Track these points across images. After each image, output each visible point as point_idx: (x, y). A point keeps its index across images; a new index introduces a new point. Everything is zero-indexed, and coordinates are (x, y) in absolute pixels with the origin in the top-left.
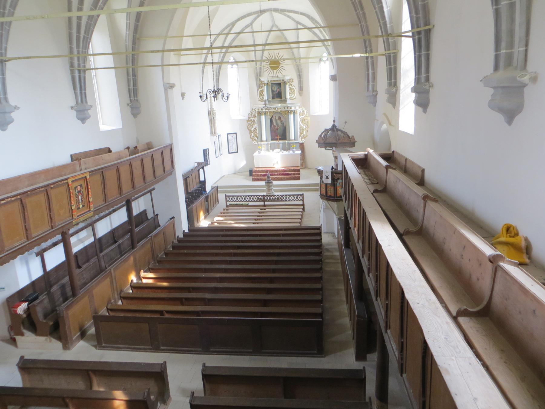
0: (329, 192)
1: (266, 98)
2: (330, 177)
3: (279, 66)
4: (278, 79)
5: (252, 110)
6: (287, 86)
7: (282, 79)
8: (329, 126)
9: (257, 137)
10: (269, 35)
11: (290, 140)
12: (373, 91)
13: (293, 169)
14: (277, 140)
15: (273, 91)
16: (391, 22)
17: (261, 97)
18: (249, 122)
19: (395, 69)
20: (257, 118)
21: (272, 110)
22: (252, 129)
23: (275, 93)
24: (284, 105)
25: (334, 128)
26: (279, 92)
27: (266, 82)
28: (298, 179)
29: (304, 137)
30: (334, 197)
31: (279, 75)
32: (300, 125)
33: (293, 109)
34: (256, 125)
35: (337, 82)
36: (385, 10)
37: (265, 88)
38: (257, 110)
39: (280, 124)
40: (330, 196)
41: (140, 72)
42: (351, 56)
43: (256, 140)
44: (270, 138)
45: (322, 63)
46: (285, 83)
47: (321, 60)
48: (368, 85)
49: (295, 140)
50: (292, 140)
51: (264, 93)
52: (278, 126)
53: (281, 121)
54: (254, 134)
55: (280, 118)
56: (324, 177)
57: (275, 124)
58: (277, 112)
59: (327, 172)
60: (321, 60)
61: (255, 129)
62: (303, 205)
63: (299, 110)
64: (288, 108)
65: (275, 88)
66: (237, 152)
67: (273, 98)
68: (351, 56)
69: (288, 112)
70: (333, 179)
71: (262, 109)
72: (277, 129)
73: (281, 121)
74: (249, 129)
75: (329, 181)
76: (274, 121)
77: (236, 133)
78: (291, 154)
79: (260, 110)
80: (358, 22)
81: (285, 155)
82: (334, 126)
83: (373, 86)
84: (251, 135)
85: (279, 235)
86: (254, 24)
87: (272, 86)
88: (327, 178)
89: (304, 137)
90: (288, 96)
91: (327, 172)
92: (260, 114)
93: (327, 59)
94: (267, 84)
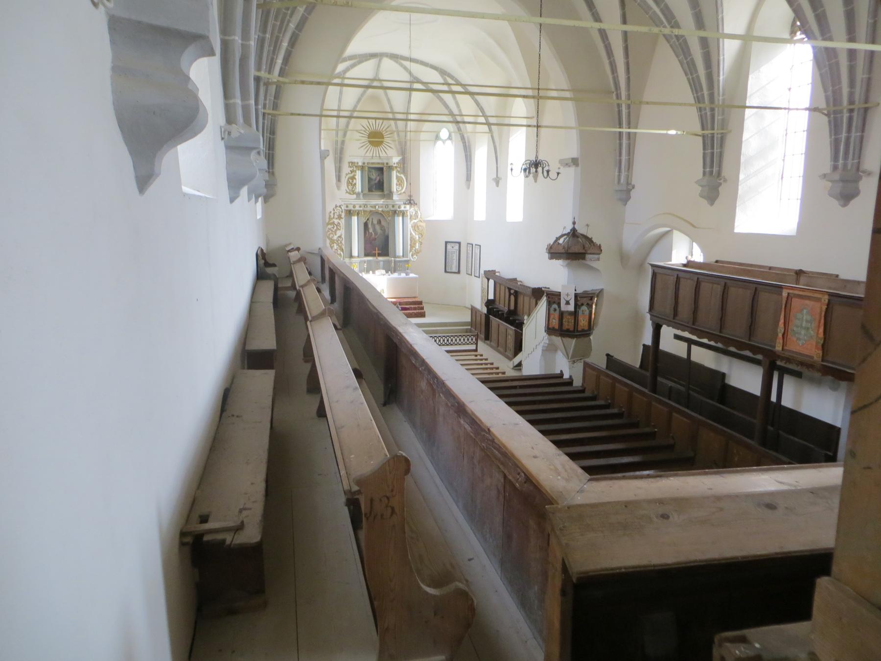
0: (565, 323)
1: (358, 188)
2: (572, 302)
3: (382, 142)
4: (379, 161)
6: (394, 174)
7: (385, 161)
8: (568, 230)
10: (364, 92)
11: (395, 257)
12: (628, 184)
13: (410, 300)
14: (374, 255)
15: (370, 179)
16: (723, 95)
17: (350, 187)
18: (330, 226)
19: (721, 155)
20: (343, 221)
21: (369, 209)
22: (335, 237)
23: (373, 183)
24: (389, 202)
25: (574, 233)
27: (360, 164)
28: (423, 315)
29: (417, 252)
30: (574, 331)
31: (383, 154)
33: (402, 208)
34: (342, 232)
35: (579, 169)
36: (721, 78)
37: (358, 174)
39: (379, 231)
40: (568, 330)
41: (282, 125)
42: (665, 132)
44: (363, 254)
45: (439, 143)
46: (390, 168)
47: (437, 138)
48: (619, 176)
50: (399, 257)
53: (382, 227)
54: (338, 245)
55: (379, 222)
56: (563, 302)
57: (371, 231)
58: (377, 213)
59: (568, 295)
61: (340, 237)
62: (476, 350)
64: (393, 206)
65: (375, 176)
67: (370, 190)
68: (665, 132)
70: (576, 305)
71: (354, 207)
72: (375, 239)
73: (382, 227)
75: (571, 308)
76: (370, 226)
78: (404, 278)
79: (351, 207)
80: (613, 89)
81: (396, 279)
82: (574, 230)
83: (628, 178)
85: (515, 387)
87: (369, 171)
88: (568, 303)
89: (417, 252)
90: (394, 188)
91: (568, 295)
92: (349, 213)
93: (450, 138)
94: (362, 168)
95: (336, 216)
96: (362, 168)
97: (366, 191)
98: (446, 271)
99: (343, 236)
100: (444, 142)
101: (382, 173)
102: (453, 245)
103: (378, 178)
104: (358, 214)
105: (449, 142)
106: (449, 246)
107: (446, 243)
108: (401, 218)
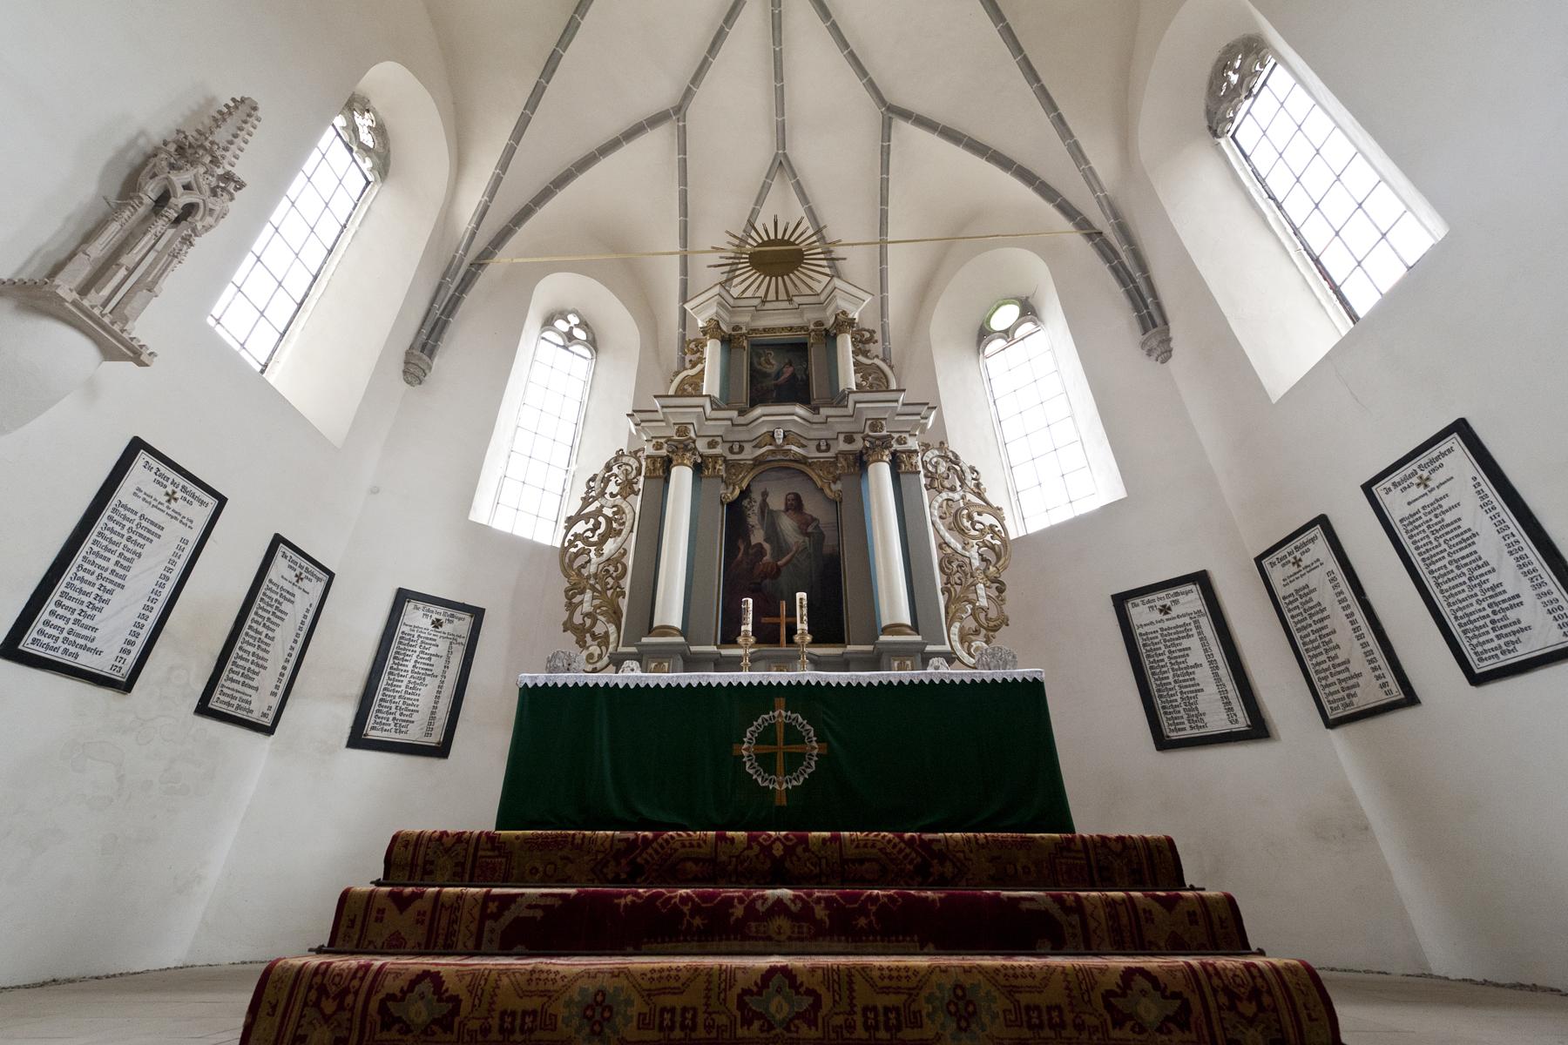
9: (615, 616)
11: (873, 628)
15: (755, 375)
18: (580, 527)
21: (749, 454)
22: (592, 569)
23: (770, 383)
26: (793, 376)
43: (603, 640)
49: (915, 627)
53: (806, 525)
55: (795, 505)
57: (758, 537)
60: (984, 334)
61: (617, 560)
65: (773, 364)
66: (441, 750)
69: (860, 463)
73: (806, 525)
76: (753, 519)
77: (477, 614)
84: (571, 607)
86: (694, 110)
92: (662, 469)
93: (1029, 310)
95: (613, 488)
96: (728, 342)
103: (788, 371)
104: (698, 469)
105: (1028, 327)
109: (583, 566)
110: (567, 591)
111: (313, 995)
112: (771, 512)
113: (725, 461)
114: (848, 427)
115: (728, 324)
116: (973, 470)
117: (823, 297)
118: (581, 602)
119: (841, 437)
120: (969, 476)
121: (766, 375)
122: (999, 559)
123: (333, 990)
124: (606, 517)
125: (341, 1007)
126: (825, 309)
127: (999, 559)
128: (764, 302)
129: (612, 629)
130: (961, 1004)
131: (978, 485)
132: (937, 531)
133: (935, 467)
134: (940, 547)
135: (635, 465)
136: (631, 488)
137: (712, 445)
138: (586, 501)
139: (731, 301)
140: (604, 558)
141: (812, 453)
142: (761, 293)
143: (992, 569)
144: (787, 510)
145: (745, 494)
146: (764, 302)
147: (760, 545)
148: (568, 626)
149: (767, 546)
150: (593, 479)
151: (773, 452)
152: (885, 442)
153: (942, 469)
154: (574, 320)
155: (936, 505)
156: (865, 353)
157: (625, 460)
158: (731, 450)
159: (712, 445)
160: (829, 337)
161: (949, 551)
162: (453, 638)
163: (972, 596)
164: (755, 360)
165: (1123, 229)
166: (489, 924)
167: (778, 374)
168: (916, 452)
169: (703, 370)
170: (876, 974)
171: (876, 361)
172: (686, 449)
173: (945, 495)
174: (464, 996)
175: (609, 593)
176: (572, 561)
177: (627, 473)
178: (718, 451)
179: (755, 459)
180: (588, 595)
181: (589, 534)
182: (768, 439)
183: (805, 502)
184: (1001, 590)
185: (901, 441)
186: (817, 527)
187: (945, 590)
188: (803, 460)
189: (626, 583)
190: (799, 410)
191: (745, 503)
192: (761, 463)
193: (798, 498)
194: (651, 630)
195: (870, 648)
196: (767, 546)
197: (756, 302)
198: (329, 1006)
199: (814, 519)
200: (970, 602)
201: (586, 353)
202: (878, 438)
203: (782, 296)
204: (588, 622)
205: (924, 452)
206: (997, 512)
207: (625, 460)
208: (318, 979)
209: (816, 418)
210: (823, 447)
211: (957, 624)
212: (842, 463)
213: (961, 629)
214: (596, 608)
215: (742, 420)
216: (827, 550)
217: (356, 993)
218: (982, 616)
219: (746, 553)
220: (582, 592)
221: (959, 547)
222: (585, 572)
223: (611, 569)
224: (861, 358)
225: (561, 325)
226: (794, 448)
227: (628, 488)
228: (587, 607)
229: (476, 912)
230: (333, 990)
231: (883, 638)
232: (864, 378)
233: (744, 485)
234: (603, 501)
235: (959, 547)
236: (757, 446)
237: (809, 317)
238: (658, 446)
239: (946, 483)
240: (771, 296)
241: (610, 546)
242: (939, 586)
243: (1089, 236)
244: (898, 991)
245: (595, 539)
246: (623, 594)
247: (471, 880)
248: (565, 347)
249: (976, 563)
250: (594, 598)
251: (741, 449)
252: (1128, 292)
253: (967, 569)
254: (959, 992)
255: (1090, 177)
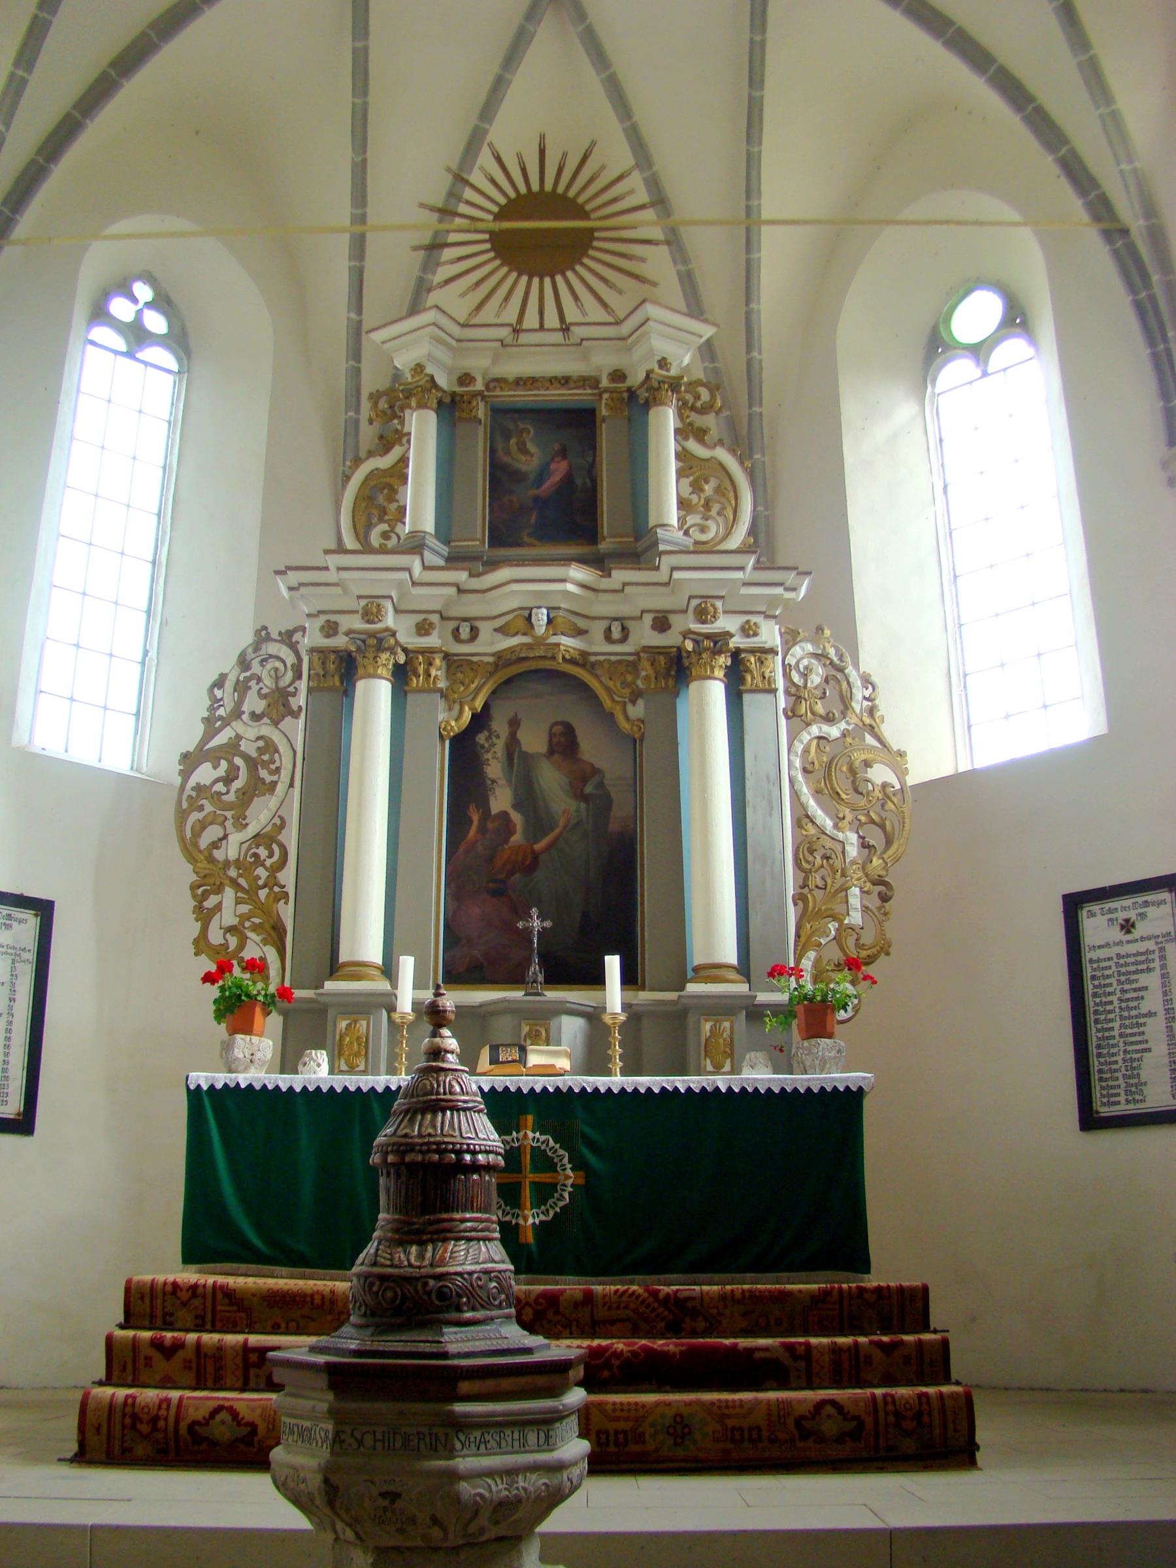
5: (262, 636)
6: (665, 421)
9: (276, 933)
14: (515, 978)
15: (501, 477)
18: (205, 774)
20: (297, 728)
21: (490, 644)
22: (231, 850)
26: (568, 479)
32: (802, 818)
33: (726, 623)
34: (282, 806)
37: (422, 428)
38: (312, 638)
45: (956, 372)
49: (744, 968)
51: (409, 495)
52: (539, 822)
53: (583, 778)
54: (248, 895)
55: (564, 744)
57: (501, 800)
60: (936, 346)
63: (793, 662)
64: (661, 624)
65: (531, 454)
69: (678, 669)
72: (530, 863)
73: (583, 778)
74: (189, 849)
76: (494, 769)
77: (44, 909)
84: (205, 916)
93: (1016, 319)
95: (253, 703)
96: (451, 408)
97: (477, 538)
98: (1090, 1120)
99: (291, 838)
100: (979, 351)
101: (590, 442)
102: (1125, 907)
103: (560, 469)
104: (401, 676)
105: (1014, 348)
106: (1097, 927)
107: (1074, 904)
108: (716, 692)
109: (215, 845)
110: (194, 887)
111: (128, 1421)
112: (525, 756)
113: (447, 656)
114: (660, 601)
115: (450, 371)
116: (867, 681)
117: (625, 329)
118: (218, 907)
119: (648, 619)
120: (859, 693)
121: (517, 476)
122: (889, 843)
123: (145, 1418)
124: (246, 758)
125: (155, 1429)
126: (629, 349)
127: (889, 843)
128: (517, 331)
129: (271, 955)
130: (679, 1428)
131: (871, 711)
132: (795, 795)
133: (805, 676)
134: (798, 824)
135: (290, 659)
136: (286, 705)
137: (423, 629)
138: (212, 724)
139: (456, 331)
140: (251, 830)
141: (599, 646)
142: (510, 314)
143: (876, 861)
144: (551, 752)
145: (480, 720)
146: (517, 331)
147: (504, 815)
148: (201, 944)
149: (516, 817)
150: (219, 683)
151: (529, 646)
152: (719, 641)
153: (816, 679)
154: (143, 292)
155: (799, 747)
156: (700, 434)
157: (272, 648)
158: (456, 632)
159: (423, 629)
160: (637, 402)
161: (812, 830)
162: (15, 954)
163: (839, 908)
164: (500, 447)
165: (1157, 236)
166: (253, 1371)
167: (541, 478)
168: (772, 651)
169: (404, 460)
170: (609, 1407)
171: (722, 454)
172: (380, 647)
173: (815, 730)
174: (259, 1422)
175: (263, 894)
176: (197, 834)
177: (277, 678)
178: (432, 641)
179: (498, 655)
180: (229, 893)
181: (220, 787)
182: (521, 624)
183: (578, 732)
184: (885, 898)
185: (748, 630)
186: (601, 785)
187: (799, 898)
188: (583, 660)
189: (288, 877)
190: (578, 573)
191: (481, 738)
192: (509, 663)
193: (569, 731)
194: (334, 967)
195: (671, 996)
196: (516, 817)
197: (504, 333)
198: (144, 1428)
199: (596, 771)
200: (834, 918)
201: (169, 360)
202: (708, 636)
203: (552, 320)
204: (233, 942)
205: (787, 647)
206: (897, 760)
207: (272, 648)
208: (128, 1409)
209: (605, 583)
210: (616, 633)
211: (812, 955)
212: (646, 670)
213: (817, 964)
214: (243, 918)
215: (475, 584)
216: (614, 826)
217: (166, 1419)
218: (850, 942)
219: (482, 829)
220: (219, 890)
221: (828, 824)
222: (219, 855)
223: (263, 852)
224: (692, 445)
225: (121, 308)
226: (566, 641)
227: (279, 705)
228: (228, 917)
229: (239, 1361)
230: (145, 1418)
231: (692, 988)
232: (697, 488)
233: (479, 704)
234: (238, 727)
235: (828, 824)
236: (502, 630)
237: (602, 362)
238: (331, 629)
239: (820, 708)
240: (531, 320)
241: (260, 816)
242: (790, 892)
243: (1108, 236)
244: (627, 1419)
245: (231, 797)
246: (286, 895)
247: (213, 1325)
248: (130, 355)
249: (853, 851)
250: (238, 901)
251: (474, 633)
252: (1155, 356)
253: (838, 864)
254: (678, 1419)
255: (1114, 124)
